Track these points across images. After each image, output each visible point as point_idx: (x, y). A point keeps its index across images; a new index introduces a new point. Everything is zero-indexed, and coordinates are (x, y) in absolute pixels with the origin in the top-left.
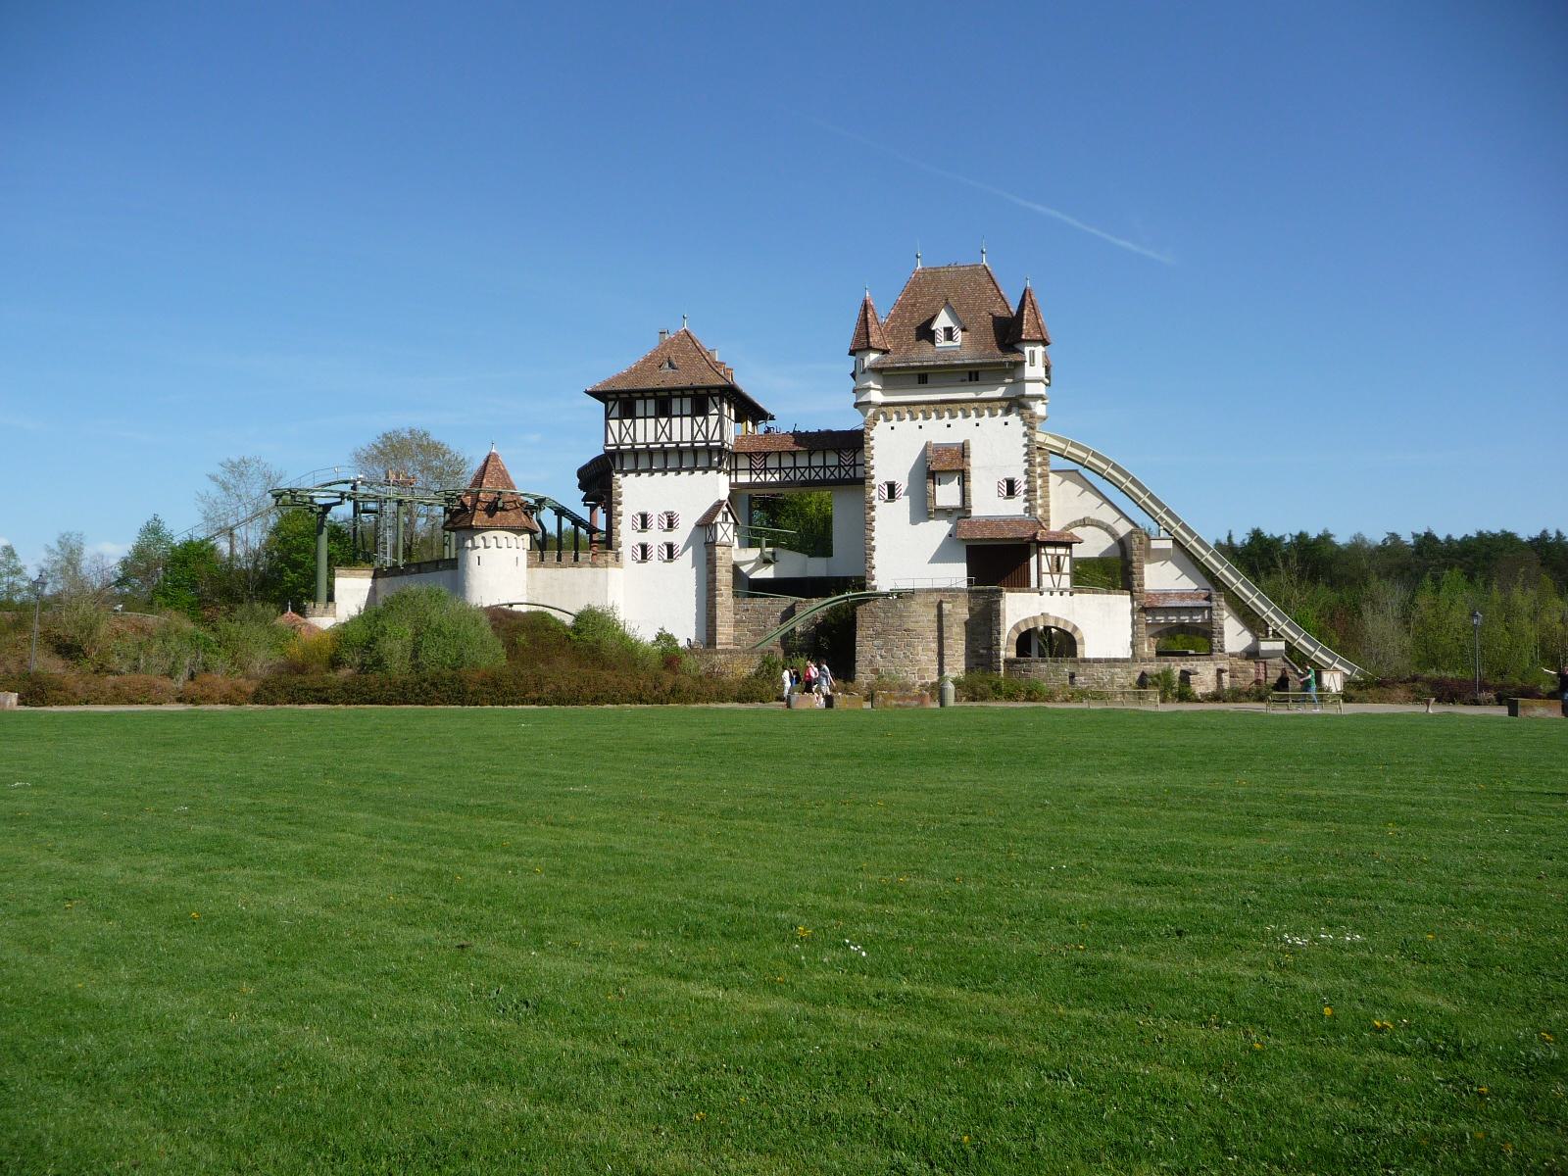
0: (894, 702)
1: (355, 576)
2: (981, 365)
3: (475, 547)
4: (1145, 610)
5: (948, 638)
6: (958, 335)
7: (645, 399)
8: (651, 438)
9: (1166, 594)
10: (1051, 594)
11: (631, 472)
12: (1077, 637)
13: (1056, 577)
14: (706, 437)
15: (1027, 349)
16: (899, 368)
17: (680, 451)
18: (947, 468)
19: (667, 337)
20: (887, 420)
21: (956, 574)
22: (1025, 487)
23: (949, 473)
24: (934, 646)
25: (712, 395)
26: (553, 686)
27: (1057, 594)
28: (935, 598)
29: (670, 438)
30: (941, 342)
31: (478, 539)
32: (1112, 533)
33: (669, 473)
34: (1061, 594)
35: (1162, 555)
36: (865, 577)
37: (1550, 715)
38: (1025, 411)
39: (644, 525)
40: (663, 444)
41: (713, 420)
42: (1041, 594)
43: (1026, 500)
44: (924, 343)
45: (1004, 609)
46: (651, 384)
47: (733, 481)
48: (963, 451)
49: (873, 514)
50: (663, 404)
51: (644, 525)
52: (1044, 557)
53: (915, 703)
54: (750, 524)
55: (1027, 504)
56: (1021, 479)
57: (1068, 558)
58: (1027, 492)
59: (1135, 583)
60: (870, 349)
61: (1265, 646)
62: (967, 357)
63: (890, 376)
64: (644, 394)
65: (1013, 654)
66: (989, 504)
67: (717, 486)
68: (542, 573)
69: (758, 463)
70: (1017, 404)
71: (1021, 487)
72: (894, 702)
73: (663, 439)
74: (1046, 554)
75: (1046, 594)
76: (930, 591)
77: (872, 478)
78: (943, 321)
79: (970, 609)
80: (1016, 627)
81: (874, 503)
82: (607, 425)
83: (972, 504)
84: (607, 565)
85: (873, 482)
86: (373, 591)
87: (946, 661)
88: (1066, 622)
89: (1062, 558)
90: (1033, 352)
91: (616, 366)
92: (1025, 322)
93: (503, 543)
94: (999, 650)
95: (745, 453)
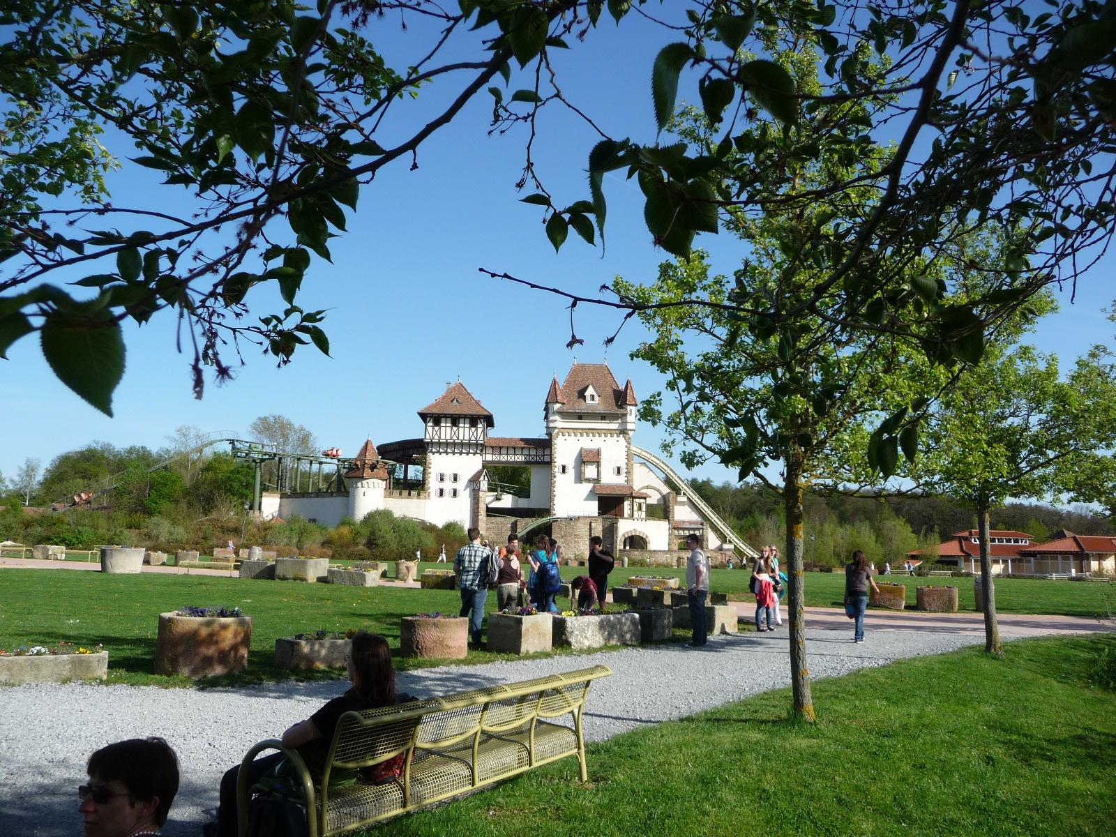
4: (674, 528)
6: (596, 398)
8: (448, 437)
9: (683, 522)
17: (462, 445)
19: (451, 386)
21: (593, 508)
23: (591, 463)
28: (588, 521)
30: (589, 401)
35: (682, 503)
39: (442, 480)
41: (480, 430)
44: (581, 400)
48: (598, 453)
50: (455, 421)
51: (442, 480)
60: (557, 402)
62: (601, 410)
63: (565, 415)
64: (446, 416)
66: (609, 478)
68: (390, 500)
69: (497, 451)
70: (623, 432)
71: (624, 470)
73: (455, 438)
76: (586, 517)
78: (590, 391)
86: (280, 506)
93: (376, 485)
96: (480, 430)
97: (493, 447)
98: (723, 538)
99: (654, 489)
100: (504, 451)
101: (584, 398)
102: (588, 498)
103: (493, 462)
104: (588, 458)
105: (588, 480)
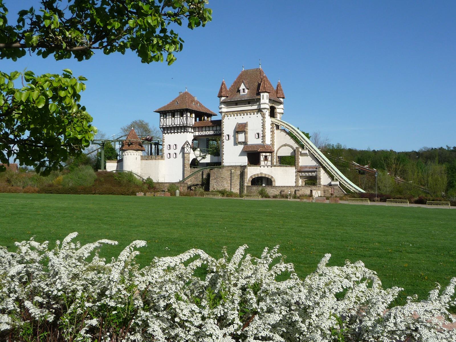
0: (159, 195)
1: (112, 162)
2: (251, 99)
3: (125, 155)
4: (299, 172)
5: (232, 180)
7: (169, 113)
8: (170, 124)
9: (306, 167)
10: (264, 167)
11: (167, 133)
12: (272, 180)
13: (266, 162)
14: (183, 123)
15: (262, 94)
16: (229, 102)
18: (241, 130)
20: (227, 117)
22: (262, 135)
24: (229, 182)
25: (184, 111)
26: (98, 191)
27: (266, 167)
29: (175, 124)
30: (242, 93)
31: (125, 152)
32: (293, 148)
33: (182, 133)
34: (268, 167)
35: (305, 155)
36: (221, 162)
37: (307, 201)
38: (262, 112)
40: (173, 125)
41: (185, 118)
42: (260, 167)
43: (262, 139)
45: (247, 172)
46: (170, 109)
47: (194, 135)
49: (223, 144)
50: (173, 113)
52: (262, 156)
53: (163, 195)
54: (208, 148)
55: (262, 140)
56: (261, 133)
57: (270, 156)
58: (262, 137)
59: (296, 163)
61: (333, 183)
63: (228, 104)
65: (250, 184)
66: (253, 140)
67: (189, 137)
69: (200, 129)
70: (260, 110)
71: (261, 135)
72: (159, 195)
73: (173, 124)
74: (262, 155)
75: (262, 167)
76: (229, 166)
77: (223, 133)
78: (242, 87)
79: (240, 171)
80: (251, 177)
81: (224, 141)
82: (160, 120)
83: (248, 141)
84: (158, 159)
85: (224, 135)
87: (232, 186)
88: (269, 175)
89: (268, 156)
90: (263, 95)
91: (164, 103)
92: (261, 86)
94: (244, 183)
95: (197, 127)
96: (185, 118)
97: (198, 127)
98: (332, 177)
99: (289, 146)
100: (204, 129)
101: (239, 91)
102: (241, 154)
103: (199, 136)
104: (241, 129)
105: (240, 143)
